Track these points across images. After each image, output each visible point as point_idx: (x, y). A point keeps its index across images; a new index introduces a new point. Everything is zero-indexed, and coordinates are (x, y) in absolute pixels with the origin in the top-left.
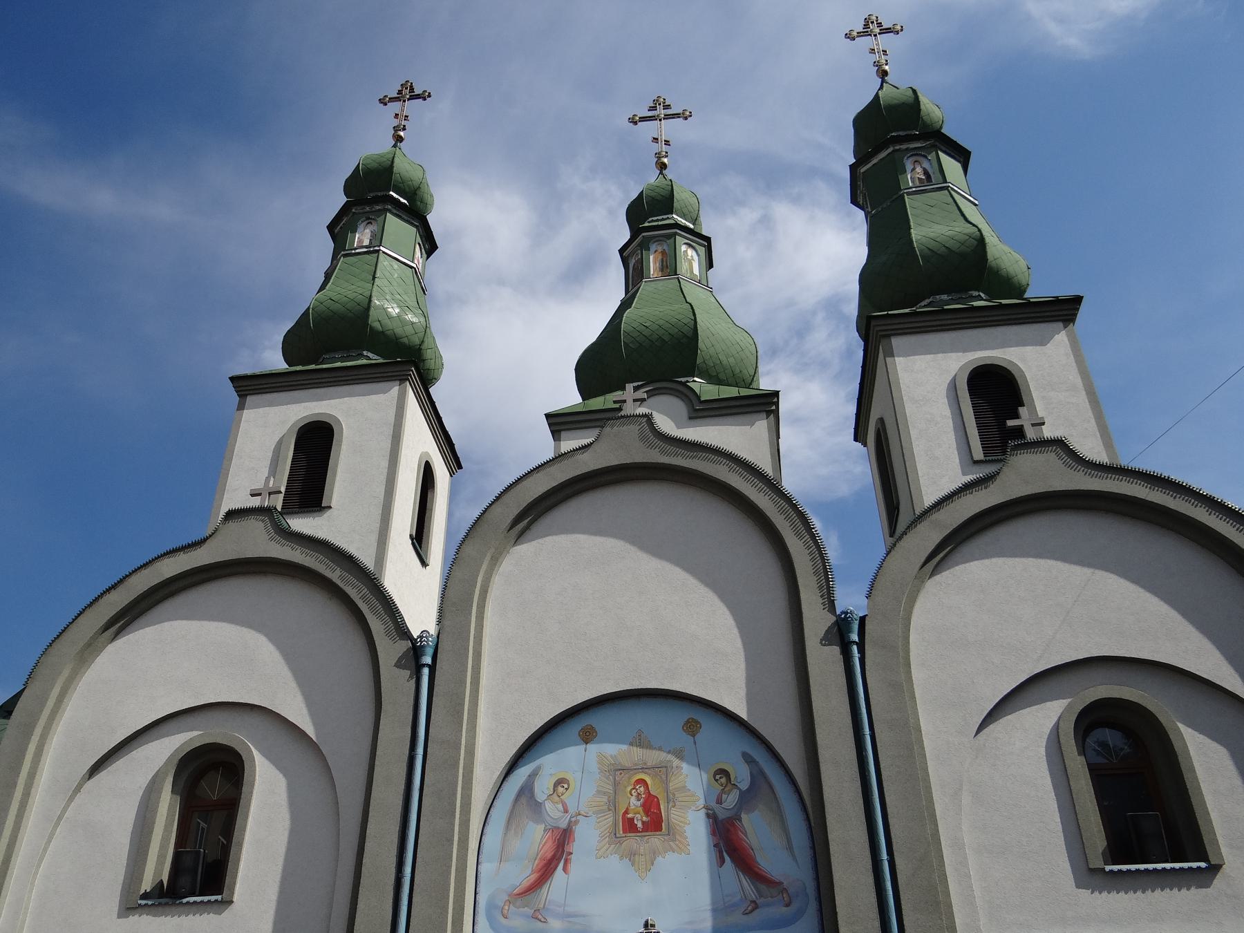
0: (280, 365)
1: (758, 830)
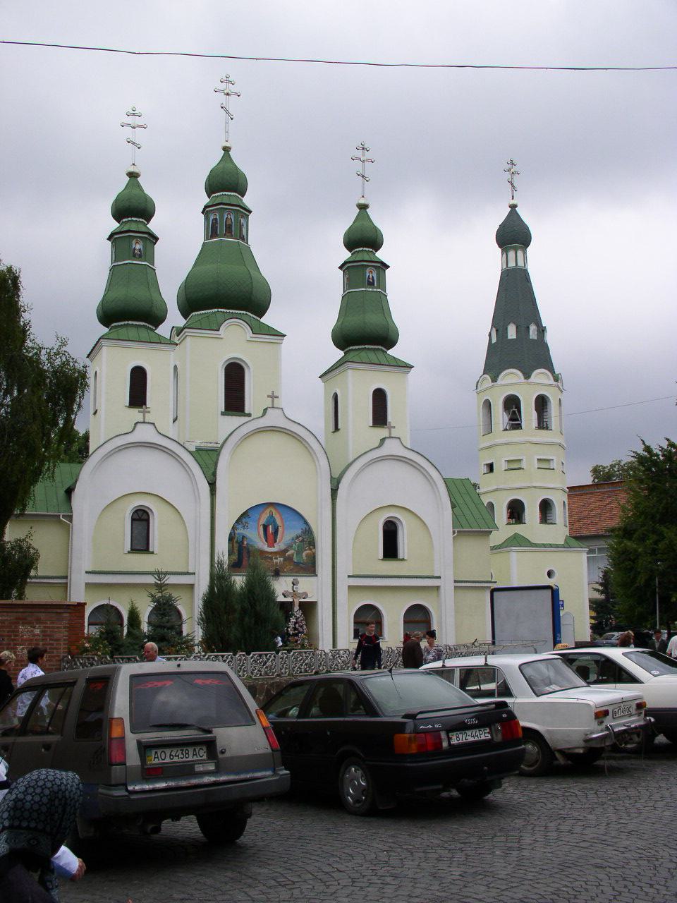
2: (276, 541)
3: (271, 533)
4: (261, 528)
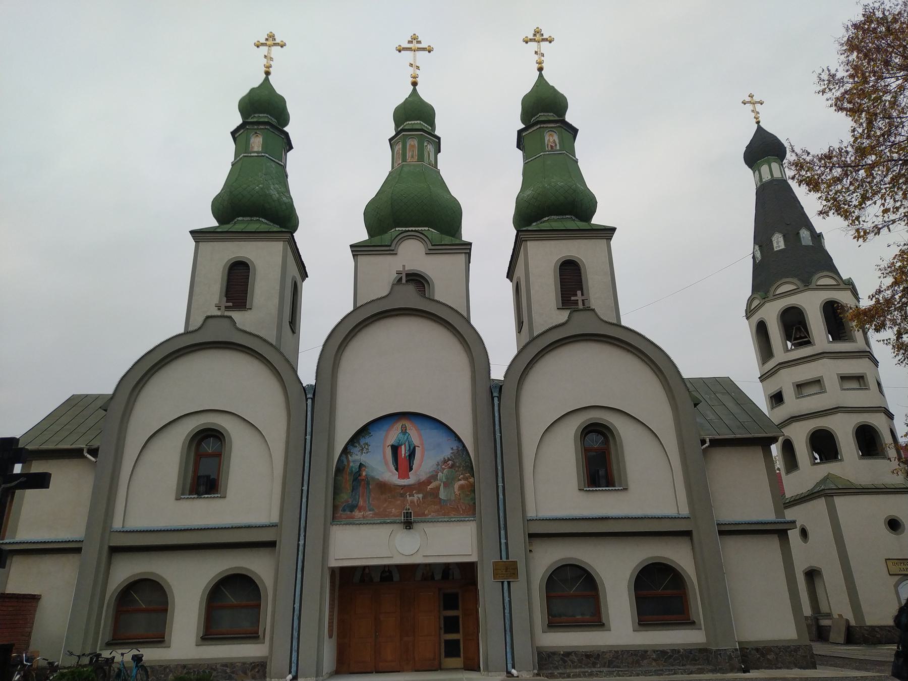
0: (214, 223)
2: (411, 469)
3: (403, 458)
4: (389, 452)
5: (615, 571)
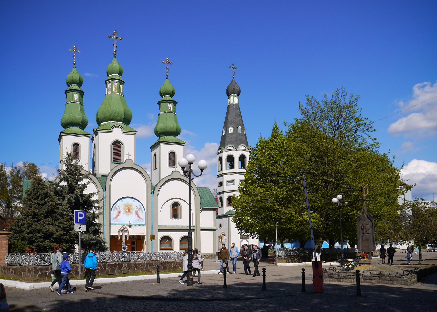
1: (140, 213)
5: (176, 237)
